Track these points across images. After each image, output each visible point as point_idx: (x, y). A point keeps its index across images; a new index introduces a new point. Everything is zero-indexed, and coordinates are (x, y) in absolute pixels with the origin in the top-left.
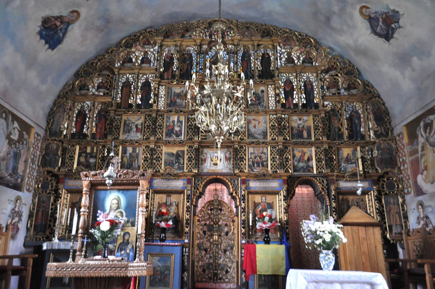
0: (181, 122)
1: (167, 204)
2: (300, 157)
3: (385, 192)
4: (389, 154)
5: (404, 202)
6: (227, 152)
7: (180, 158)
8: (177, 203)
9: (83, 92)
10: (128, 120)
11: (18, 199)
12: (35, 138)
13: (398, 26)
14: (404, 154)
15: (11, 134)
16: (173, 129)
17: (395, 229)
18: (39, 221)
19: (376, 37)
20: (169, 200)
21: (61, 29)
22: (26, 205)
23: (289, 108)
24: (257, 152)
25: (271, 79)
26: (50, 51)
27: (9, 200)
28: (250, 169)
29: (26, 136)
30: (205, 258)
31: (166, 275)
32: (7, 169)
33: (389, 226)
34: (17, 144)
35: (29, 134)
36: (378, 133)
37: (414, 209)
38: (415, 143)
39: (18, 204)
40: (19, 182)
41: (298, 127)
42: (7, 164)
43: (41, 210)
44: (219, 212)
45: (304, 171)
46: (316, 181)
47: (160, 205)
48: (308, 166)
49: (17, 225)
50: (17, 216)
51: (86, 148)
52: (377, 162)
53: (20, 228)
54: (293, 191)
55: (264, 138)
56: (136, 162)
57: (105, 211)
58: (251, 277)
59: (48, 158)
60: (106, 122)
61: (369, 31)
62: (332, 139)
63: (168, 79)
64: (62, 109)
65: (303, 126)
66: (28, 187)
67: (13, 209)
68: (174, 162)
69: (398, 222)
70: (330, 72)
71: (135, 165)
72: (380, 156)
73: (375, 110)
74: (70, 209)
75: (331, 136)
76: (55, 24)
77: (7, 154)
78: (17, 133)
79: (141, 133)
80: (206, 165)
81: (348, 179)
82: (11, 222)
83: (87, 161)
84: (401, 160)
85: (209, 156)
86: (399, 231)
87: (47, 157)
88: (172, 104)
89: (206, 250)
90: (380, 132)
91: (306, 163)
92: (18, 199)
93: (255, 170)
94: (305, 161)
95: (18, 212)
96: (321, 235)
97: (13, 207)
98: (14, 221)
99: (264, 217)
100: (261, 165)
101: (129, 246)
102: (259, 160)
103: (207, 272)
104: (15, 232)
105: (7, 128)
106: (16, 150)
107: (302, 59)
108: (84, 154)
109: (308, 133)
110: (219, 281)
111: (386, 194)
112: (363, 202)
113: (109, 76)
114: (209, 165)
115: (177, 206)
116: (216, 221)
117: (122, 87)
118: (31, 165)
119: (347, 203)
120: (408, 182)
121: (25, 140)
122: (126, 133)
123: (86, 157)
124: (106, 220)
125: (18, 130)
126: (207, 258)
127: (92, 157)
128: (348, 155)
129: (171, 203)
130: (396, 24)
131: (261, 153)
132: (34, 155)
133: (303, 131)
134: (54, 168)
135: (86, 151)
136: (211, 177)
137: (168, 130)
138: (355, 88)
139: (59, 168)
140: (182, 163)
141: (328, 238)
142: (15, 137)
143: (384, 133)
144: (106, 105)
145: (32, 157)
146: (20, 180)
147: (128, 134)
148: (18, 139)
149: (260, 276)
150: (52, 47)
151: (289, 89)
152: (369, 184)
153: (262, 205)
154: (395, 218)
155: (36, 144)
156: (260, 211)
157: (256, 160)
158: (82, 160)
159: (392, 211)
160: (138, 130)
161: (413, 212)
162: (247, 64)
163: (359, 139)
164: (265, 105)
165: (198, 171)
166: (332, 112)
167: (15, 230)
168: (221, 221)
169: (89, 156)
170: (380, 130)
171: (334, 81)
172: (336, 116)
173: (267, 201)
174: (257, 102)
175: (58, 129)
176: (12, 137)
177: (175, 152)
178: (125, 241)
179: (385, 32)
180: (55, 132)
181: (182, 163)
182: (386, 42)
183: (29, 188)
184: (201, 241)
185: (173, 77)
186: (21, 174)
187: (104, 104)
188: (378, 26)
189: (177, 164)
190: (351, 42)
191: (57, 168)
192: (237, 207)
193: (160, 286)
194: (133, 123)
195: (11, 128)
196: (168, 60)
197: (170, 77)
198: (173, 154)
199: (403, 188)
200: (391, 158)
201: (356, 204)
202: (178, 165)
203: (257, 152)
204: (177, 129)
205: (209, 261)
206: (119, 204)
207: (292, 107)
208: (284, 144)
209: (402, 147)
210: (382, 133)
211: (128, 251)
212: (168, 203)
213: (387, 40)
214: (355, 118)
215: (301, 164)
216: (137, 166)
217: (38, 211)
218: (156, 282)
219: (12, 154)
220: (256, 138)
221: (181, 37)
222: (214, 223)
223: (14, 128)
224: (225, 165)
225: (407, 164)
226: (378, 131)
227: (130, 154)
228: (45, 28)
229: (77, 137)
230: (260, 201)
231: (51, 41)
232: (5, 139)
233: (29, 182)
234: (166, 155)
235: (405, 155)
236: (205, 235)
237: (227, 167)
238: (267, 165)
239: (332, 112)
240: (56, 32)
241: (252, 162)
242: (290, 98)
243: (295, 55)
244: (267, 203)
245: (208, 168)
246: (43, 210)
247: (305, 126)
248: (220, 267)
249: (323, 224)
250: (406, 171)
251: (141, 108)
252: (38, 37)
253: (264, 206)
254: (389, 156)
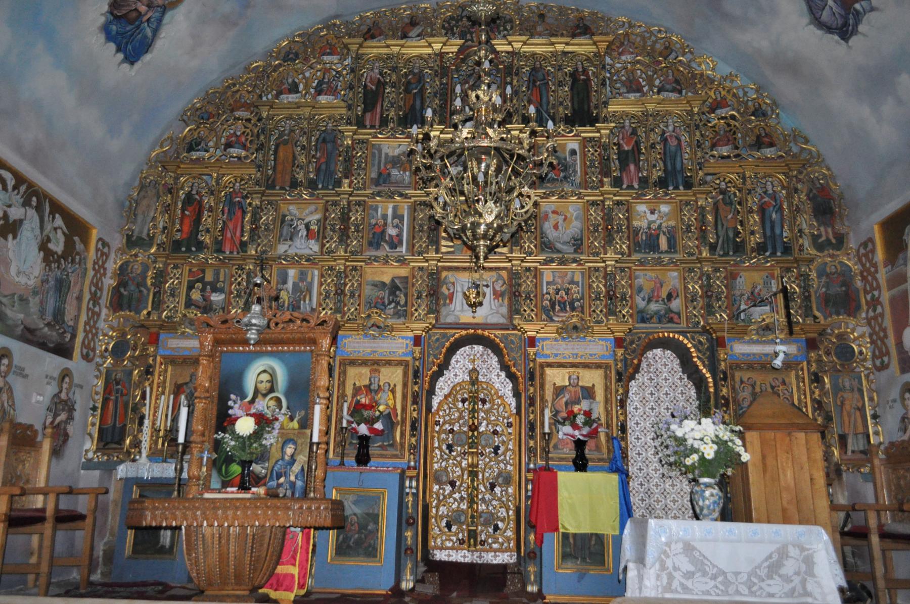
0: (401, 218)
1: (372, 387)
2: (653, 291)
4: (844, 284)
6: (497, 281)
7: (398, 293)
8: (392, 386)
9: (195, 155)
10: (291, 214)
11: (66, 374)
12: (97, 250)
13: (867, 8)
14: (875, 285)
15: (49, 240)
16: (383, 232)
17: (853, 444)
18: (110, 422)
19: (819, 32)
20: (377, 379)
21: (148, 20)
22: (81, 387)
23: (630, 187)
24: (560, 281)
25: (592, 125)
26: (126, 66)
27: (47, 377)
28: (544, 317)
29: (79, 246)
30: (451, 500)
31: (370, 532)
32: (42, 312)
34: (62, 261)
35: (85, 241)
36: (820, 241)
37: (894, 401)
38: (901, 262)
39: (65, 386)
40: (67, 340)
41: (649, 228)
42: (41, 303)
43: (113, 398)
44: (481, 407)
45: (660, 322)
46: (686, 341)
47: (357, 391)
48: (670, 310)
49: (65, 429)
50: (63, 410)
51: (203, 271)
52: (817, 303)
53: (70, 434)
54: (636, 361)
55: (576, 251)
56: (307, 302)
57: (246, 397)
58: (547, 536)
59: (125, 293)
60: (244, 218)
61: (806, 19)
62: (721, 253)
63: (372, 127)
64: (154, 191)
65: (660, 226)
66: (85, 351)
67: (57, 395)
68: (387, 302)
69: (860, 429)
70: (718, 111)
71: (305, 307)
72: (824, 290)
73: (814, 191)
74: (172, 397)
75: (718, 249)
76: (136, 10)
77: (43, 282)
78: (62, 239)
79: (317, 240)
80: (452, 306)
81: (755, 338)
82: (52, 423)
83: (205, 299)
84: (869, 297)
85: (459, 289)
86: (862, 448)
87: (122, 290)
88: (381, 181)
89: (452, 484)
90: (824, 238)
91: (665, 304)
92: (66, 374)
93: (554, 318)
94: (663, 300)
95: (66, 401)
96: (696, 446)
97: (57, 390)
98: (58, 419)
99: (575, 416)
100: (568, 309)
101: (293, 468)
102: (565, 297)
103: (454, 528)
104: (60, 442)
105: (42, 228)
106: (59, 273)
107: (657, 82)
108: (199, 285)
109: (669, 240)
110: (479, 547)
112: (785, 387)
113: (249, 120)
114: (458, 308)
115: (393, 391)
116: (473, 423)
117: (277, 146)
118: (91, 306)
119: (750, 388)
120: (883, 343)
121: (78, 254)
122: (286, 240)
123: (203, 290)
124: (247, 415)
125: (64, 233)
126: (455, 500)
127: (215, 290)
128: (754, 287)
129: (379, 386)
130: (863, 3)
131: (569, 284)
132: (96, 286)
133: (658, 235)
134: (138, 312)
135: (204, 277)
136: (464, 332)
137: (374, 234)
138: (771, 145)
139: (149, 313)
140: (402, 303)
141: (710, 452)
142: (58, 246)
143: (834, 241)
144: (243, 182)
145: (93, 289)
146: (68, 336)
147: (290, 243)
148: (63, 252)
149: (566, 536)
150: (131, 59)
151: (630, 148)
152: (799, 350)
153: (570, 392)
154: (853, 419)
155: (100, 263)
156: (566, 404)
157: (558, 297)
158: (196, 295)
160: (310, 234)
161: (891, 407)
162: (541, 95)
163: (779, 254)
164: (578, 181)
165: (437, 319)
166: (721, 197)
167: (62, 438)
168: (485, 423)
169: (208, 287)
170: (823, 233)
171: (728, 129)
172: (731, 204)
173: (580, 384)
174: (562, 175)
175: (145, 232)
176: (51, 246)
177: (387, 279)
178: (287, 458)
179: (840, 22)
180: (140, 238)
181: (402, 303)
182: (842, 42)
183: (88, 355)
184: (444, 464)
185: (384, 122)
186: (71, 323)
187: (239, 180)
188: (824, 9)
189: (393, 305)
190: (764, 44)
191: (145, 312)
192: (517, 394)
193: (358, 555)
194: (299, 219)
195: (48, 227)
196: (374, 87)
197: (377, 124)
198: (384, 284)
200: (847, 294)
201: (769, 390)
202: (395, 308)
203: (560, 281)
204: (392, 231)
205: (459, 507)
206: (272, 381)
207: (636, 186)
208: (619, 265)
209: (872, 269)
210: (828, 240)
211: (292, 478)
212: (374, 387)
213: (843, 39)
214: (771, 208)
215: (654, 307)
216: (308, 309)
217: (106, 401)
218: (349, 547)
219: (52, 283)
220: (559, 251)
221: (402, 39)
222: (470, 427)
223: (55, 229)
224: (493, 307)
225: (882, 306)
226: (819, 236)
227: (295, 284)
228: (117, 17)
229: (184, 249)
230: (567, 384)
231: (130, 47)
232: (37, 251)
233: (86, 342)
234: (369, 287)
235: (878, 287)
236: (450, 453)
237: (497, 313)
238: (582, 307)
239: (721, 197)
240: (138, 27)
241: (550, 301)
242: (632, 167)
243: (644, 76)
244: (582, 387)
245: (456, 313)
246: (117, 397)
247: (664, 225)
248: (482, 519)
249: (700, 423)
250: (880, 319)
251: (316, 188)
252: (102, 37)
253: (575, 392)
254: (844, 289)
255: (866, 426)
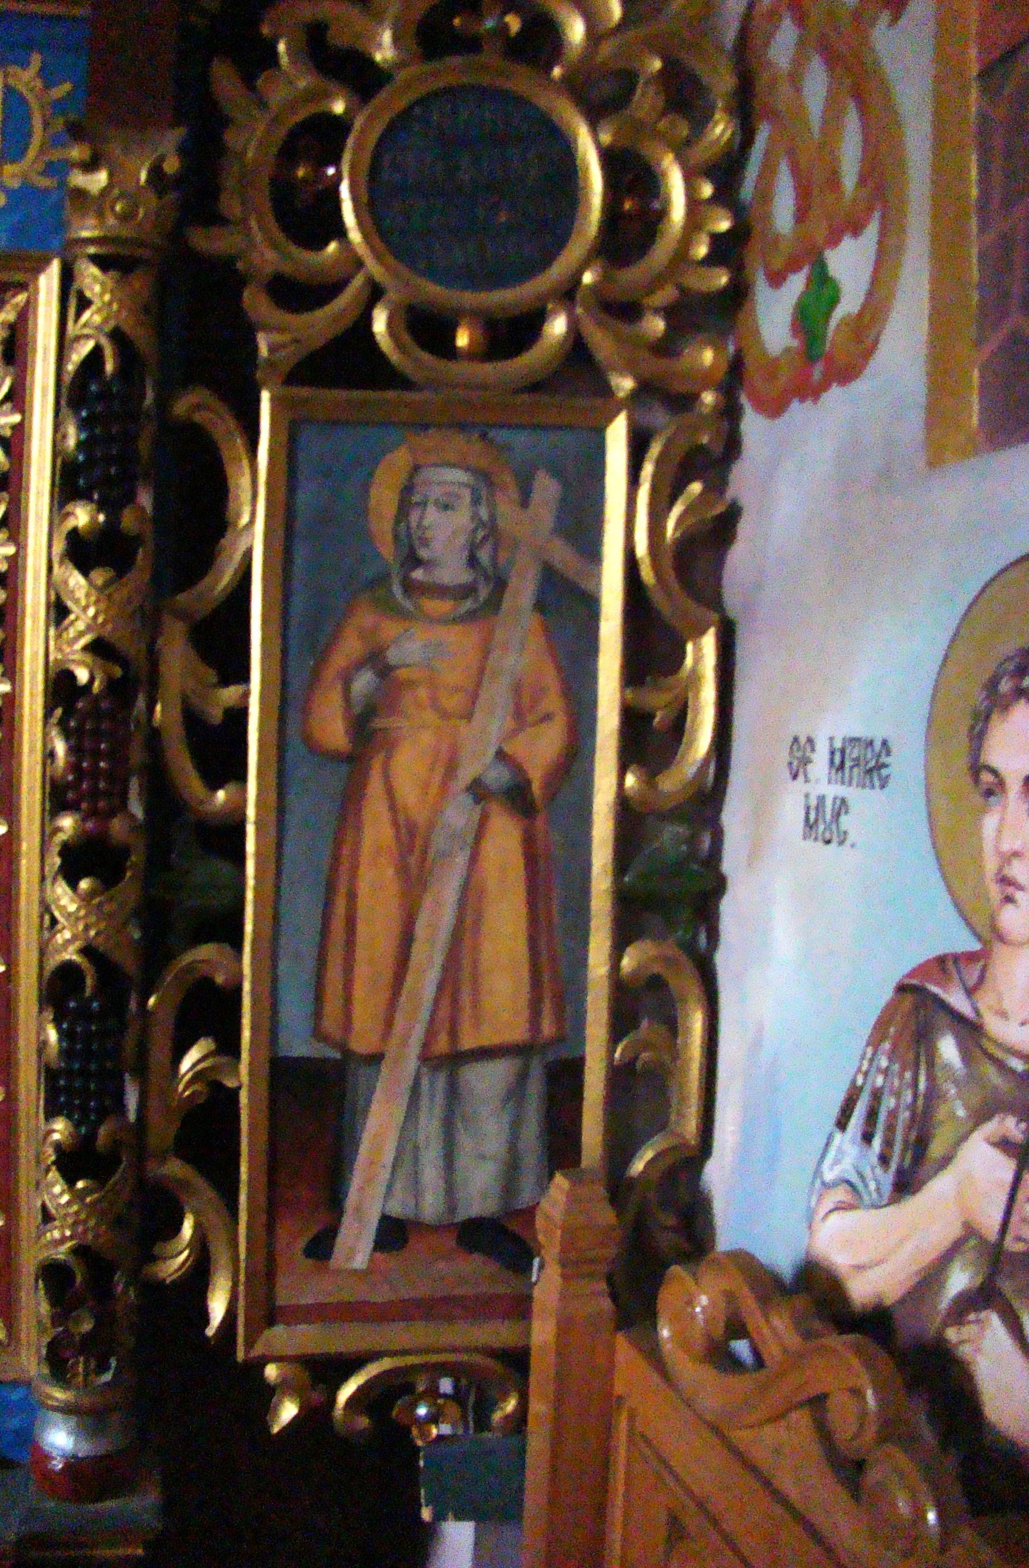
3: (322, 322)
5: (699, 556)
33: (283, 1074)
37: (864, 761)
69: (502, 1005)
86: (479, 1192)
111: (348, 360)
159: (408, 766)
161: (823, 824)
199: (727, 250)
255: (553, 974)
